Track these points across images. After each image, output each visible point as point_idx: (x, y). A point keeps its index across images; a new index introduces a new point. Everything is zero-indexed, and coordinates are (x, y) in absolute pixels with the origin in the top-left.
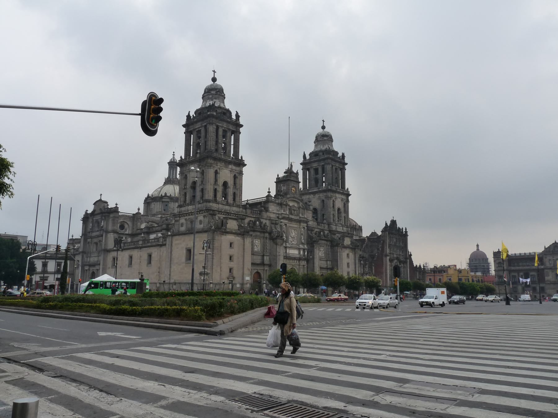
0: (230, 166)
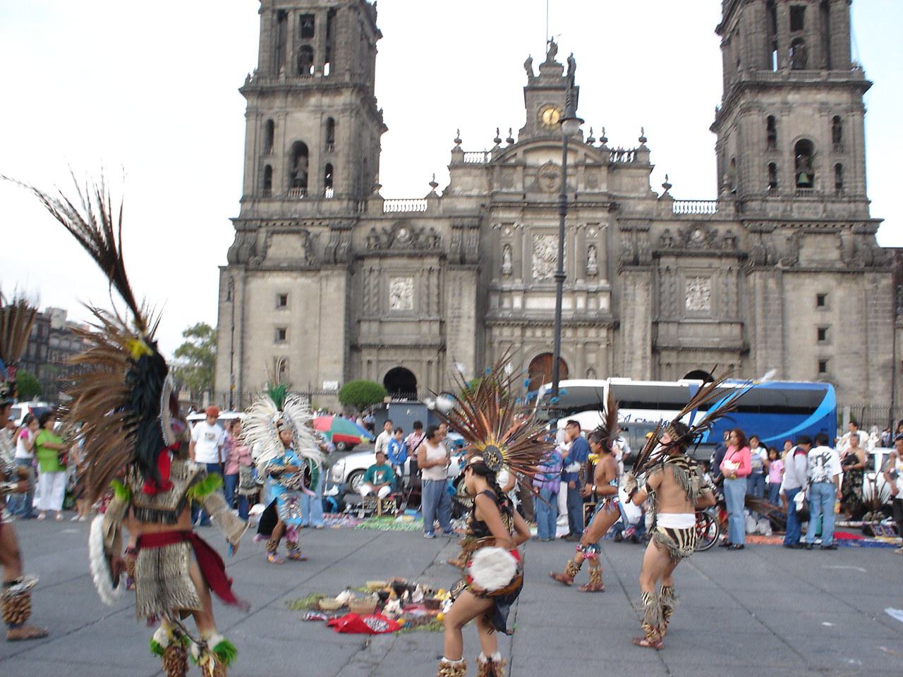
0: (313, 100)
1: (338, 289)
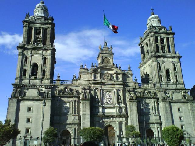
0: (40, 52)
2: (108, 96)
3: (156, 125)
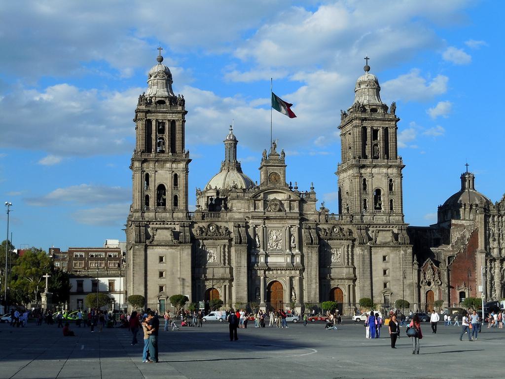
0: (168, 165)
1: (187, 255)
2: (275, 237)
3: (346, 281)
